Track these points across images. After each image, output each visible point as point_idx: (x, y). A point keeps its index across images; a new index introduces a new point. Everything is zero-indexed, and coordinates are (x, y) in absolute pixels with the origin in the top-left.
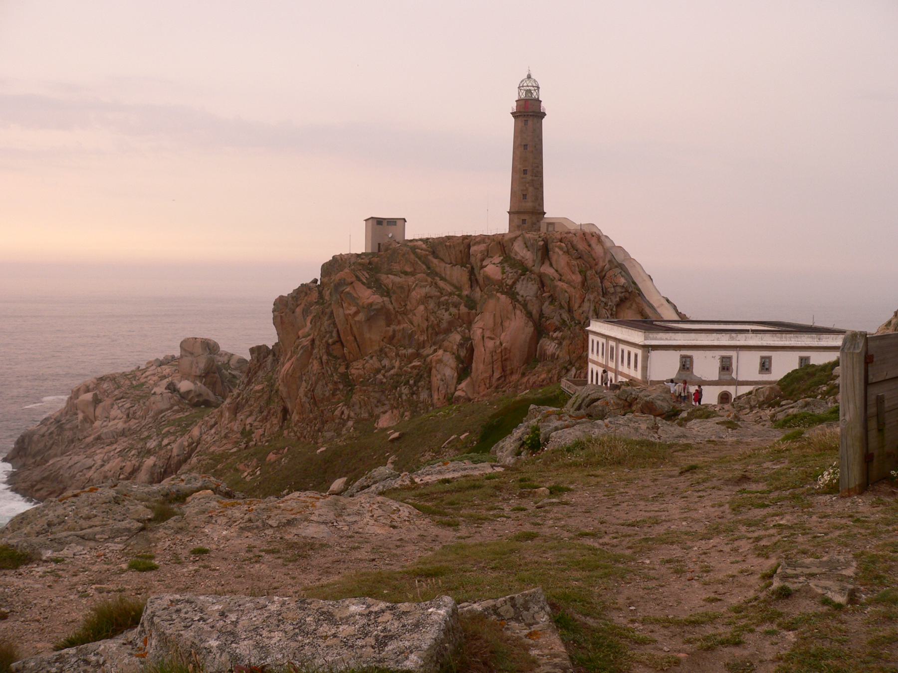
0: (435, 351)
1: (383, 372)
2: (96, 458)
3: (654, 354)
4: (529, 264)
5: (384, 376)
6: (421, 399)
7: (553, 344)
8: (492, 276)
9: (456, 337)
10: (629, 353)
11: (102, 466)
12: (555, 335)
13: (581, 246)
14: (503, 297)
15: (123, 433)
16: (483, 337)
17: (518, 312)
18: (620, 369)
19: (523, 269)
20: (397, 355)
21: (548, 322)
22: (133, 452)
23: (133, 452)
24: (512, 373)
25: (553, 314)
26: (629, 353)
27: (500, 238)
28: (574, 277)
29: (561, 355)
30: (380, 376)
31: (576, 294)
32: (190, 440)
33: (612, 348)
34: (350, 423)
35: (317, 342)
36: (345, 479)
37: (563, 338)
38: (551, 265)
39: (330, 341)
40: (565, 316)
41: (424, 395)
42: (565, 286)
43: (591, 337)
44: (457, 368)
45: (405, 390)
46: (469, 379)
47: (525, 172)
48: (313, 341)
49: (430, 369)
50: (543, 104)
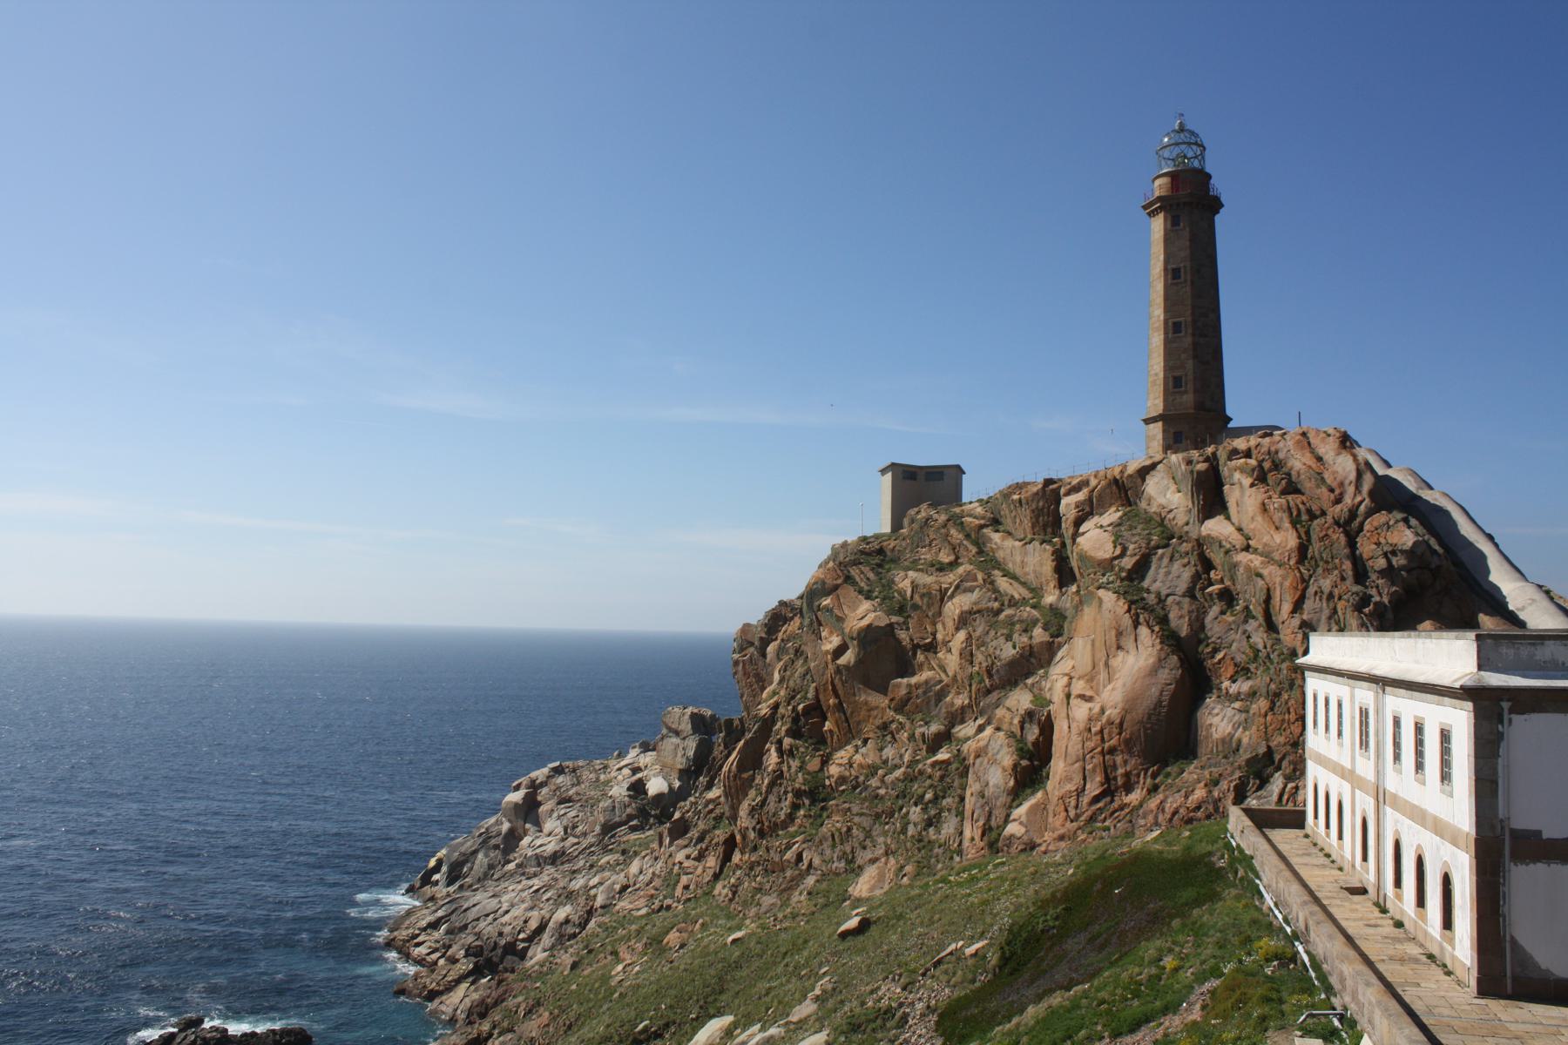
0: (981, 729)
1: (880, 772)
2: (505, 898)
3: (1523, 729)
4: (1181, 518)
5: (882, 781)
6: (942, 837)
7: (1229, 712)
8: (1092, 553)
9: (1020, 700)
10: (1419, 729)
11: (507, 912)
12: (1234, 689)
13: (1298, 462)
14: (1107, 597)
15: (555, 858)
16: (1068, 696)
17: (1144, 631)
18: (1392, 783)
19: (1165, 534)
20: (912, 737)
21: (1219, 656)
22: (548, 895)
23: (548, 895)
24: (1129, 788)
25: (1232, 636)
26: (1419, 729)
27: (1117, 472)
28: (1278, 538)
29: (1245, 740)
30: (874, 782)
31: (1280, 580)
32: (625, 881)
33: (1364, 713)
34: (810, 880)
35: (781, 710)
36: (728, 1019)
37: (1253, 694)
38: (1228, 518)
39: (801, 707)
40: (1259, 638)
41: (948, 828)
42: (1256, 561)
43: (1313, 684)
44: (1015, 766)
45: (915, 813)
46: (1039, 795)
48: (776, 707)
49: (967, 769)
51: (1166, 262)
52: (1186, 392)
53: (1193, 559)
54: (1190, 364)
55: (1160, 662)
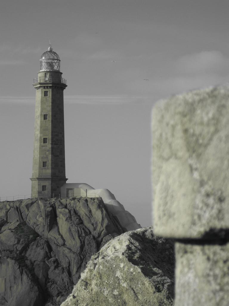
17: (25, 277)
42: (67, 251)
47: (45, 140)
50: (63, 76)
51: (42, 111)
52: (48, 169)
53: (45, 246)
54: (50, 157)
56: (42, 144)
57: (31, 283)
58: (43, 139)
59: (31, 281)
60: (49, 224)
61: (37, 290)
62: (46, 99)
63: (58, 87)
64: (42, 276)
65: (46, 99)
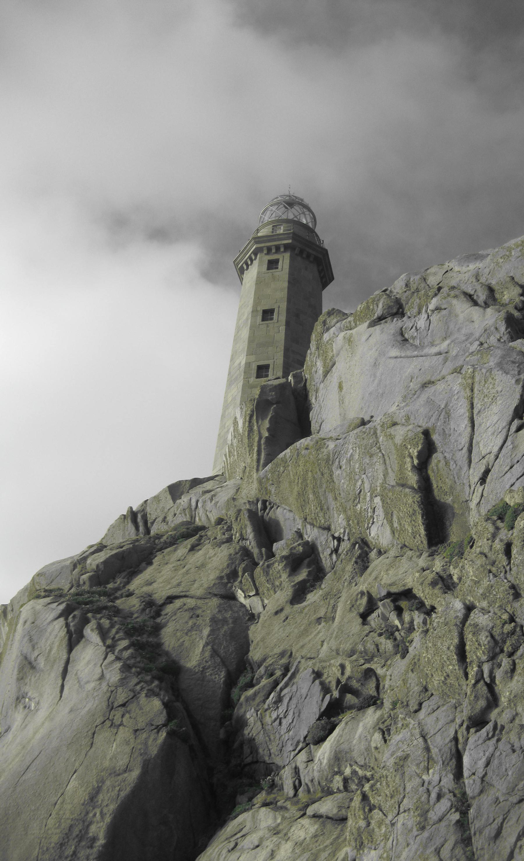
55: (113, 712)
56: (253, 380)
57: (123, 682)
58: (254, 367)
59: (126, 668)
60: (267, 434)
61: (162, 719)
62: (273, 275)
63: (308, 256)
64: (207, 654)
65: (273, 275)
